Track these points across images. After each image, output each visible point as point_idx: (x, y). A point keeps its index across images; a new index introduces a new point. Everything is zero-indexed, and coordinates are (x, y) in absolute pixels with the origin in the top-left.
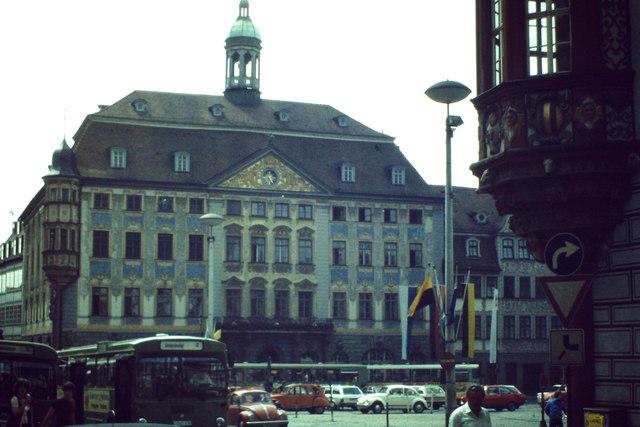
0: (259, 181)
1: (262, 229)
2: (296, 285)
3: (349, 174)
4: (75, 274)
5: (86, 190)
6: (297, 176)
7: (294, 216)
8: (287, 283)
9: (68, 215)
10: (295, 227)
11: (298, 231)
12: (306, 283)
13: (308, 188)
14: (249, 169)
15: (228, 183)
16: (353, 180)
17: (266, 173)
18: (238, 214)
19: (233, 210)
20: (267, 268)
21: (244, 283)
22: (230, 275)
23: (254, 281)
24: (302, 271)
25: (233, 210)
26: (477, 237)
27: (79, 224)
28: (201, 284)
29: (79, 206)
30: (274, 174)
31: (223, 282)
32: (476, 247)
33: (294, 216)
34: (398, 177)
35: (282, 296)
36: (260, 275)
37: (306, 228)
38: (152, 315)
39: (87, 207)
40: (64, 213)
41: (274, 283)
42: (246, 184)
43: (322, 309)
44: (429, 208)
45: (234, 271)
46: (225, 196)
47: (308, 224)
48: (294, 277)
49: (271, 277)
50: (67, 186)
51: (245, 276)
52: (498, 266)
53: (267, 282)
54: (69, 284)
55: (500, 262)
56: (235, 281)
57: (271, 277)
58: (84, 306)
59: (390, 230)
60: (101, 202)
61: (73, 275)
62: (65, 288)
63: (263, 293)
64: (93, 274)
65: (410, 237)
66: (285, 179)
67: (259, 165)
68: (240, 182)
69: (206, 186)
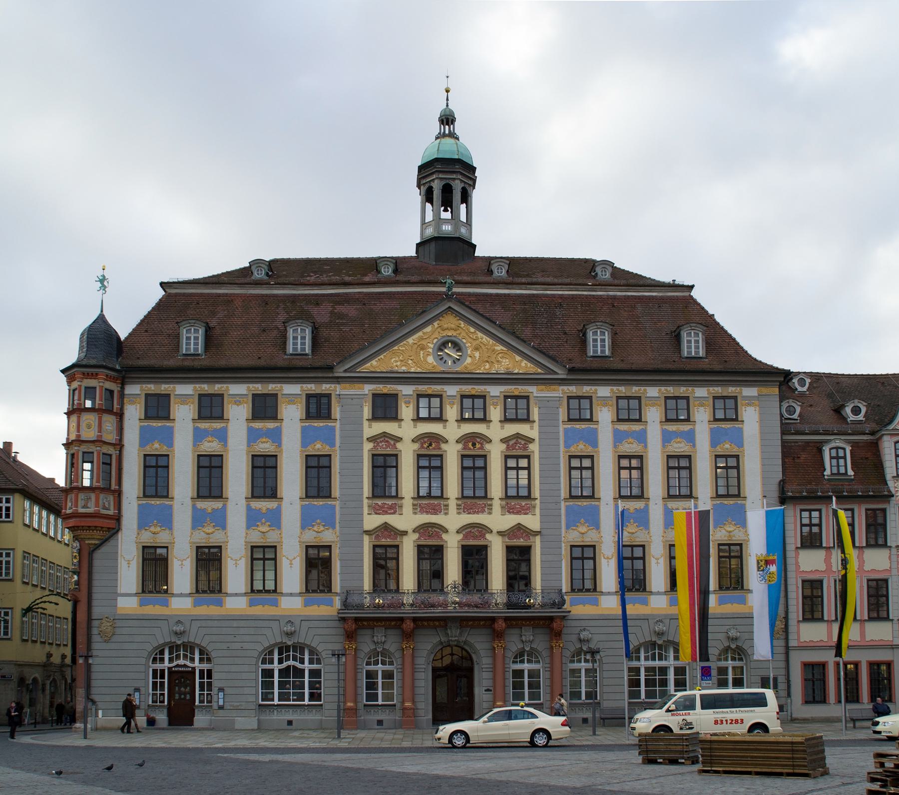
0: (430, 359)
1: (434, 439)
2: (500, 533)
3: (599, 342)
4: (112, 523)
5: (133, 389)
6: (499, 348)
7: (495, 413)
8: (483, 529)
10: (496, 431)
11: (504, 441)
13: (523, 366)
14: (410, 340)
15: (375, 365)
16: (607, 353)
17: (443, 346)
18: (394, 417)
19: (386, 408)
20: (447, 506)
21: (405, 533)
23: (424, 529)
24: (511, 510)
26: (848, 442)
27: (119, 445)
29: (120, 416)
30: (457, 346)
32: (845, 458)
33: (495, 413)
34: (693, 344)
35: (474, 559)
37: (518, 436)
39: (133, 413)
40: (89, 426)
42: (407, 365)
43: (547, 575)
44: (750, 392)
45: (386, 513)
46: (368, 389)
47: (523, 429)
48: (498, 520)
49: (453, 520)
50: (92, 383)
51: (407, 519)
52: (890, 491)
53: (446, 531)
54: (104, 541)
55: (891, 484)
56: (386, 528)
57: (453, 520)
58: (129, 575)
59: (677, 434)
60: (157, 409)
61: (111, 527)
62: (98, 547)
64: (142, 525)
65: (714, 443)
67: (431, 334)
69: (330, 368)
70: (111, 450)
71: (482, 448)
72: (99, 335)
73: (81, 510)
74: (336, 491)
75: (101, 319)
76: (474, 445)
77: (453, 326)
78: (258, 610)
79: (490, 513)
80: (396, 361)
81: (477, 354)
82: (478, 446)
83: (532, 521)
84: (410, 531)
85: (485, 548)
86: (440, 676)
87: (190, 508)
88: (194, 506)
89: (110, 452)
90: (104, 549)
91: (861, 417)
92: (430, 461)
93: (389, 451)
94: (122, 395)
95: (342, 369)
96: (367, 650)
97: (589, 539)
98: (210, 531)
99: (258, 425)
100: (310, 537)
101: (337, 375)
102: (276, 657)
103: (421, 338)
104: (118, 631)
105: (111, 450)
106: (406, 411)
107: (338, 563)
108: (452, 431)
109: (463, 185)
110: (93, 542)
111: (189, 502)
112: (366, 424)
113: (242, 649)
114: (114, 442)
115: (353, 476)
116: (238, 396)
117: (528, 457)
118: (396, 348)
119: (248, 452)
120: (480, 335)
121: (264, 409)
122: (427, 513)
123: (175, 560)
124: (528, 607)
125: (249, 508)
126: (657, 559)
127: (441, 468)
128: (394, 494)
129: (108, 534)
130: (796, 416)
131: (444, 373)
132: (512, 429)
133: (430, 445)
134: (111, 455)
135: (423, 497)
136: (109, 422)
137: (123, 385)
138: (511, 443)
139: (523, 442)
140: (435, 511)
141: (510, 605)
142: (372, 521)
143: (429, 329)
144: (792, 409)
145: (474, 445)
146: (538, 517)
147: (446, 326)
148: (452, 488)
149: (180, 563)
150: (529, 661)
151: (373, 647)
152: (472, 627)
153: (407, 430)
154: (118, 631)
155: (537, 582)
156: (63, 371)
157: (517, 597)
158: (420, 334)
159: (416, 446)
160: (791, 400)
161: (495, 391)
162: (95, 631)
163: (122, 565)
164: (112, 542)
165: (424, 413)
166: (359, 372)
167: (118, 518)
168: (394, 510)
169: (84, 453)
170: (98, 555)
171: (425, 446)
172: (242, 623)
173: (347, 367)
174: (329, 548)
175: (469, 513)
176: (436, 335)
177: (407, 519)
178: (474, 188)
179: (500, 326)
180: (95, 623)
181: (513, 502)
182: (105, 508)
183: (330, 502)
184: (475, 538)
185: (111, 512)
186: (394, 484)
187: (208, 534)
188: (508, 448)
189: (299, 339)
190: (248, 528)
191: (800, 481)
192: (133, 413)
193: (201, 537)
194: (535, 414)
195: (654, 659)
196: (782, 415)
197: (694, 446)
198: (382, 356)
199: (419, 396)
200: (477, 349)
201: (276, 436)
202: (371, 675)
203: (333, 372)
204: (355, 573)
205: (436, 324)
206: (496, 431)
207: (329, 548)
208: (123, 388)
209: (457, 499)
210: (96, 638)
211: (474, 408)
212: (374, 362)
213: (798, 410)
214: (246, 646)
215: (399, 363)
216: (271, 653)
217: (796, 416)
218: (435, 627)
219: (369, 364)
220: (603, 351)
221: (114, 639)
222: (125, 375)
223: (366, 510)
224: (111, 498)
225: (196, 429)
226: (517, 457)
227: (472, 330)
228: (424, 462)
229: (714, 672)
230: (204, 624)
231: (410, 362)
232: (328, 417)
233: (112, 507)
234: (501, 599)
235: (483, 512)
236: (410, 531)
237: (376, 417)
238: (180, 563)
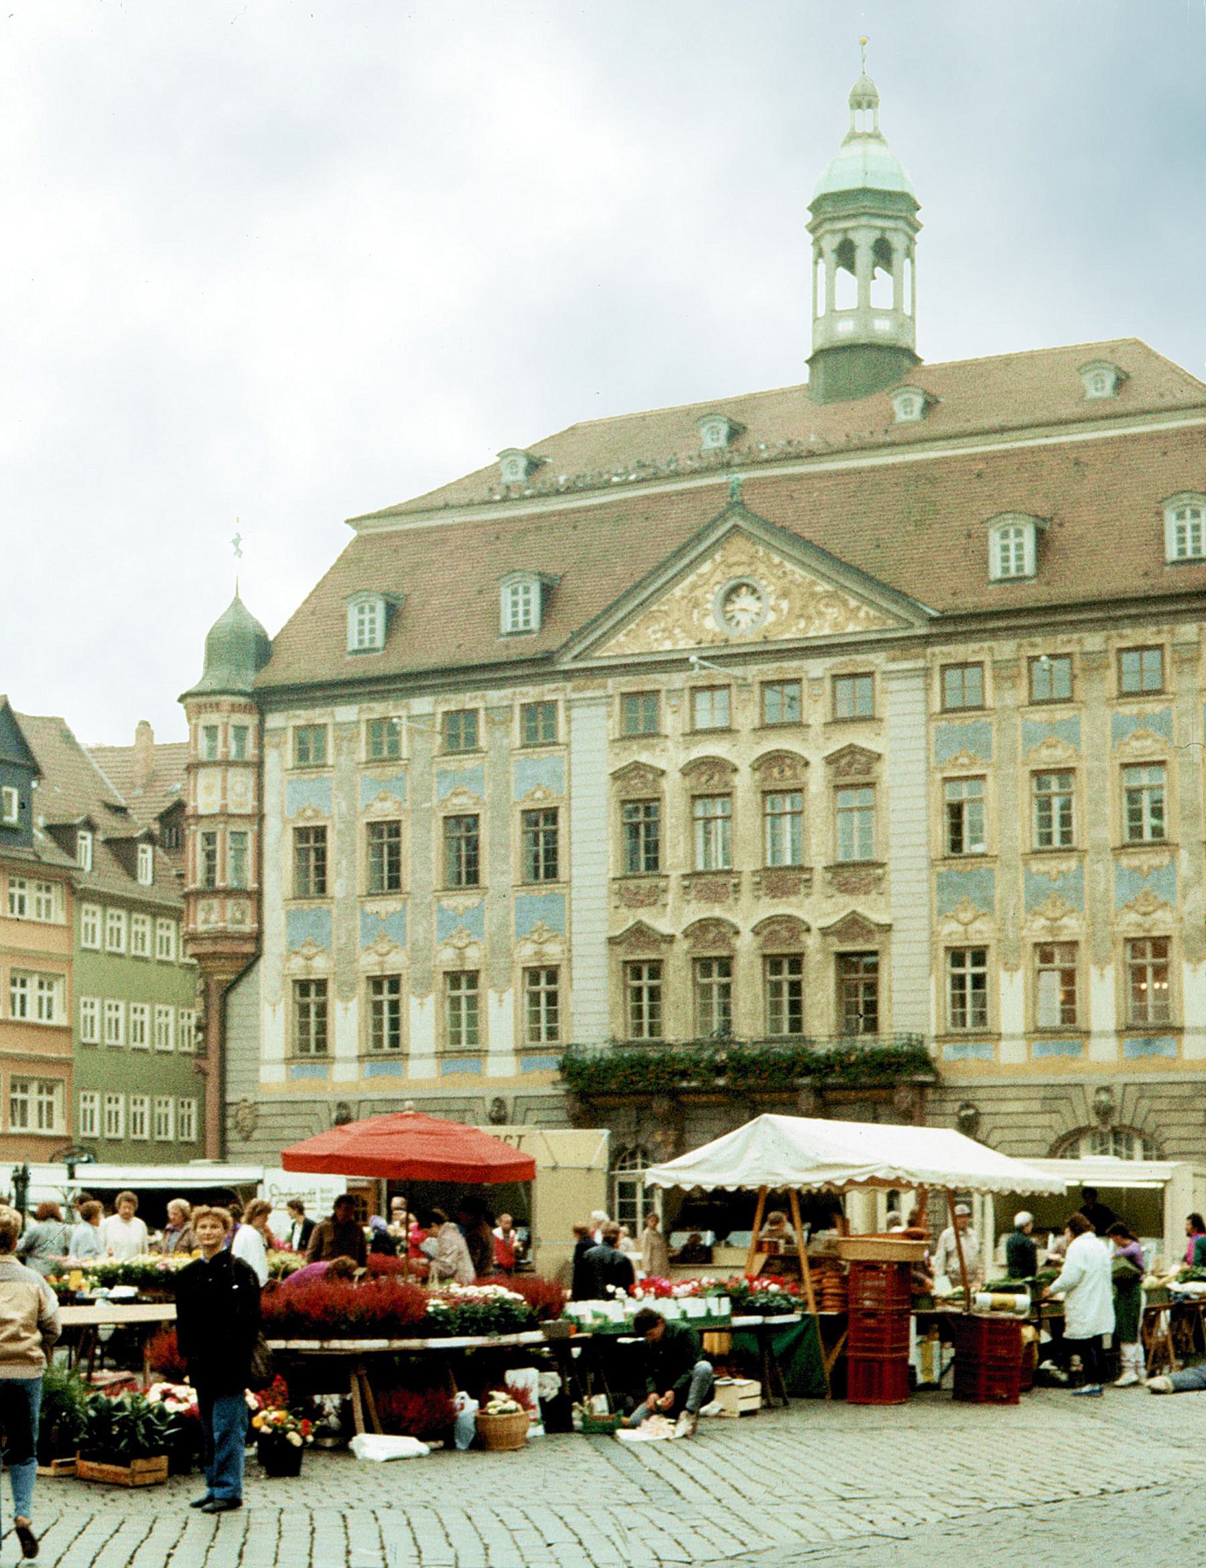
2: (825, 932)
4: (249, 948)
5: (274, 720)
6: (822, 587)
9: (217, 792)
11: (831, 760)
12: (853, 925)
14: (677, 592)
15: (623, 645)
18: (652, 733)
19: (640, 717)
22: (629, 918)
25: (640, 717)
28: (553, 952)
31: (612, 941)
36: (717, 912)
40: (209, 788)
41: (756, 931)
42: (671, 636)
47: (861, 737)
48: (819, 909)
49: (747, 913)
51: (673, 917)
56: (640, 932)
57: (747, 913)
62: (231, 987)
66: (778, 601)
67: (711, 575)
71: (795, 776)
75: (237, 602)
77: (744, 558)
80: (654, 632)
81: (785, 605)
82: (788, 773)
84: (679, 935)
90: (242, 988)
93: (645, 793)
94: (261, 730)
95: (570, 656)
98: (384, 951)
101: (566, 667)
103: (694, 587)
104: (260, 1122)
110: (224, 977)
118: (654, 608)
120: (788, 566)
129: (246, 962)
133: (712, 778)
136: (241, 781)
137: (262, 715)
138: (843, 762)
139: (863, 759)
143: (706, 568)
147: (732, 560)
154: (260, 1122)
156: (182, 699)
158: (692, 578)
159: (688, 783)
162: (230, 1123)
163: (266, 1011)
164: (252, 976)
166: (599, 658)
167: (257, 937)
168: (653, 897)
170: (233, 998)
171: (703, 779)
173: (575, 653)
176: (718, 576)
180: (231, 1111)
184: (785, 942)
188: (838, 773)
189: (517, 607)
192: (279, 760)
198: (633, 626)
200: (785, 594)
203: (553, 664)
205: (718, 557)
208: (262, 722)
210: (232, 1135)
212: (621, 637)
215: (659, 635)
220: (1020, 568)
222: (264, 700)
227: (777, 560)
231: (677, 631)
233: (248, 920)
236: (679, 935)
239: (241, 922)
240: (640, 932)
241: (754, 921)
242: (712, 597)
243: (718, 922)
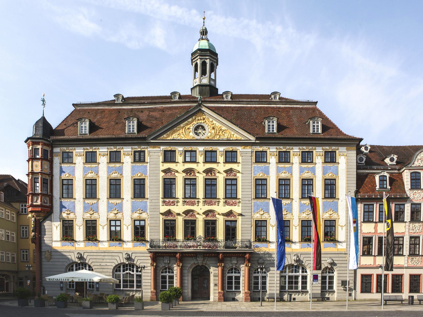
0: (191, 134)
6: (224, 128)
12: (230, 213)
35: (210, 227)
38: (106, 240)
43: (244, 233)
45: (170, 205)
46: (162, 148)
47: (234, 166)
48: (221, 208)
49: (200, 208)
51: (179, 208)
57: (200, 208)
63: (194, 222)
68: (175, 136)
70: (47, 177)
71: (215, 175)
72: (43, 124)
73: (35, 204)
74: (147, 195)
76: (211, 174)
78: (113, 249)
79: (218, 205)
81: (213, 131)
82: (213, 174)
83: (237, 209)
85: (216, 220)
86: (195, 279)
87: (82, 203)
88: (84, 202)
89: (47, 178)
91: (394, 163)
92: (190, 183)
96: (161, 266)
97: (264, 218)
98: (92, 213)
99: (112, 165)
100: (136, 215)
101: (149, 141)
102: (122, 269)
105: (47, 177)
106: (180, 158)
107: (149, 227)
108: (200, 167)
109: (211, 62)
111: (82, 200)
112: (161, 164)
113: (106, 265)
114: (48, 173)
115: (154, 189)
116: (103, 153)
117: (236, 179)
118: (175, 129)
119: (108, 178)
120: (214, 122)
121: (115, 158)
122: (189, 205)
123: (77, 226)
124: (236, 248)
125: (108, 203)
126: (296, 227)
127: (195, 185)
128: (174, 197)
130: (363, 162)
131: (197, 140)
132: (229, 166)
133: (191, 174)
134: (47, 180)
135: (187, 198)
140: (193, 204)
141: (226, 247)
142: (164, 209)
144: (362, 159)
145: (211, 174)
146: (240, 207)
148: (200, 193)
149: (79, 227)
150: (235, 273)
151: (164, 265)
152: (209, 257)
153: (179, 166)
155: (239, 237)
157: (230, 243)
159: (184, 174)
160: (361, 155)
161: (221, 149)
165: (188, 159)
168: (173, 204)
169: (35, 178)
172: (106, 254)
174: (145, 220)
175: (209, 205)
177: (179, 208)
178: (217, 65)
179: (224, 118)
181: (229, 200)
182: (44, 203)
183: (145, 200)
185: (48, 205)
186: (174, 192)
187: (91, 214)
190: (108, 212)
191: (364, 193)
193: (87, 216)
194: (240, 159)
195: (292, 272)
196: (357, 162)
197: (314, 174)
198: (169, 133)
199: (186, 151)
201: (120, 170)
202: (164, 277)
204: (155, 233)
206: (221, 167)
207: (145, 220)
209: (203, 199)
211: (210, 157)
213: (365, 159)
214: (108, 264)
216: (120, 267)
217: (363, 162)
218: (192, 257)
219: (162, 137)
221: (52, 260)
223: (161, 203)
224: (48, 199)
225: (84, 168)
226: (231, 179)
227: (211, 120)
228: (188, 182)
229: (320, 278)
230: (89, 254)
232: (144, 161)
233: (48, 202)
234: (222, 244)
235: (215, 205)
237: (165, 161)
238: (79, 227)
239: (47, 203)
240: (169, 213)
241: (203, 211)
242: (192, 127)
243: (192, 211)
